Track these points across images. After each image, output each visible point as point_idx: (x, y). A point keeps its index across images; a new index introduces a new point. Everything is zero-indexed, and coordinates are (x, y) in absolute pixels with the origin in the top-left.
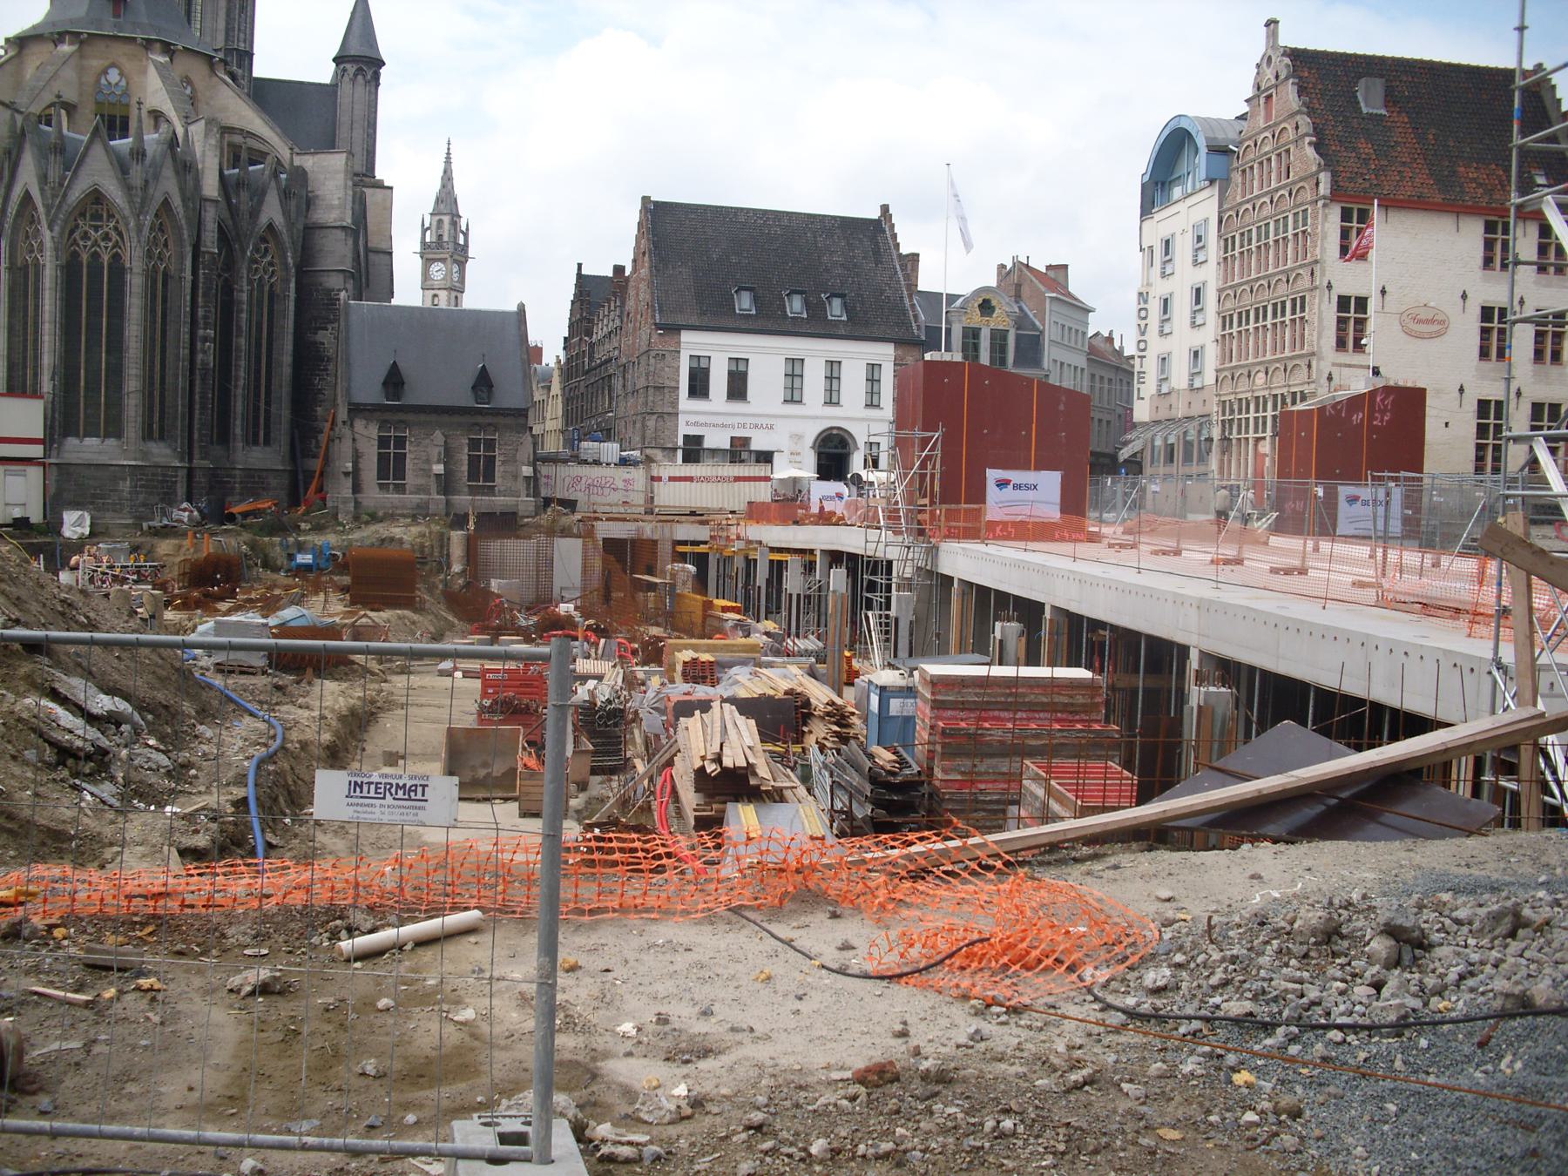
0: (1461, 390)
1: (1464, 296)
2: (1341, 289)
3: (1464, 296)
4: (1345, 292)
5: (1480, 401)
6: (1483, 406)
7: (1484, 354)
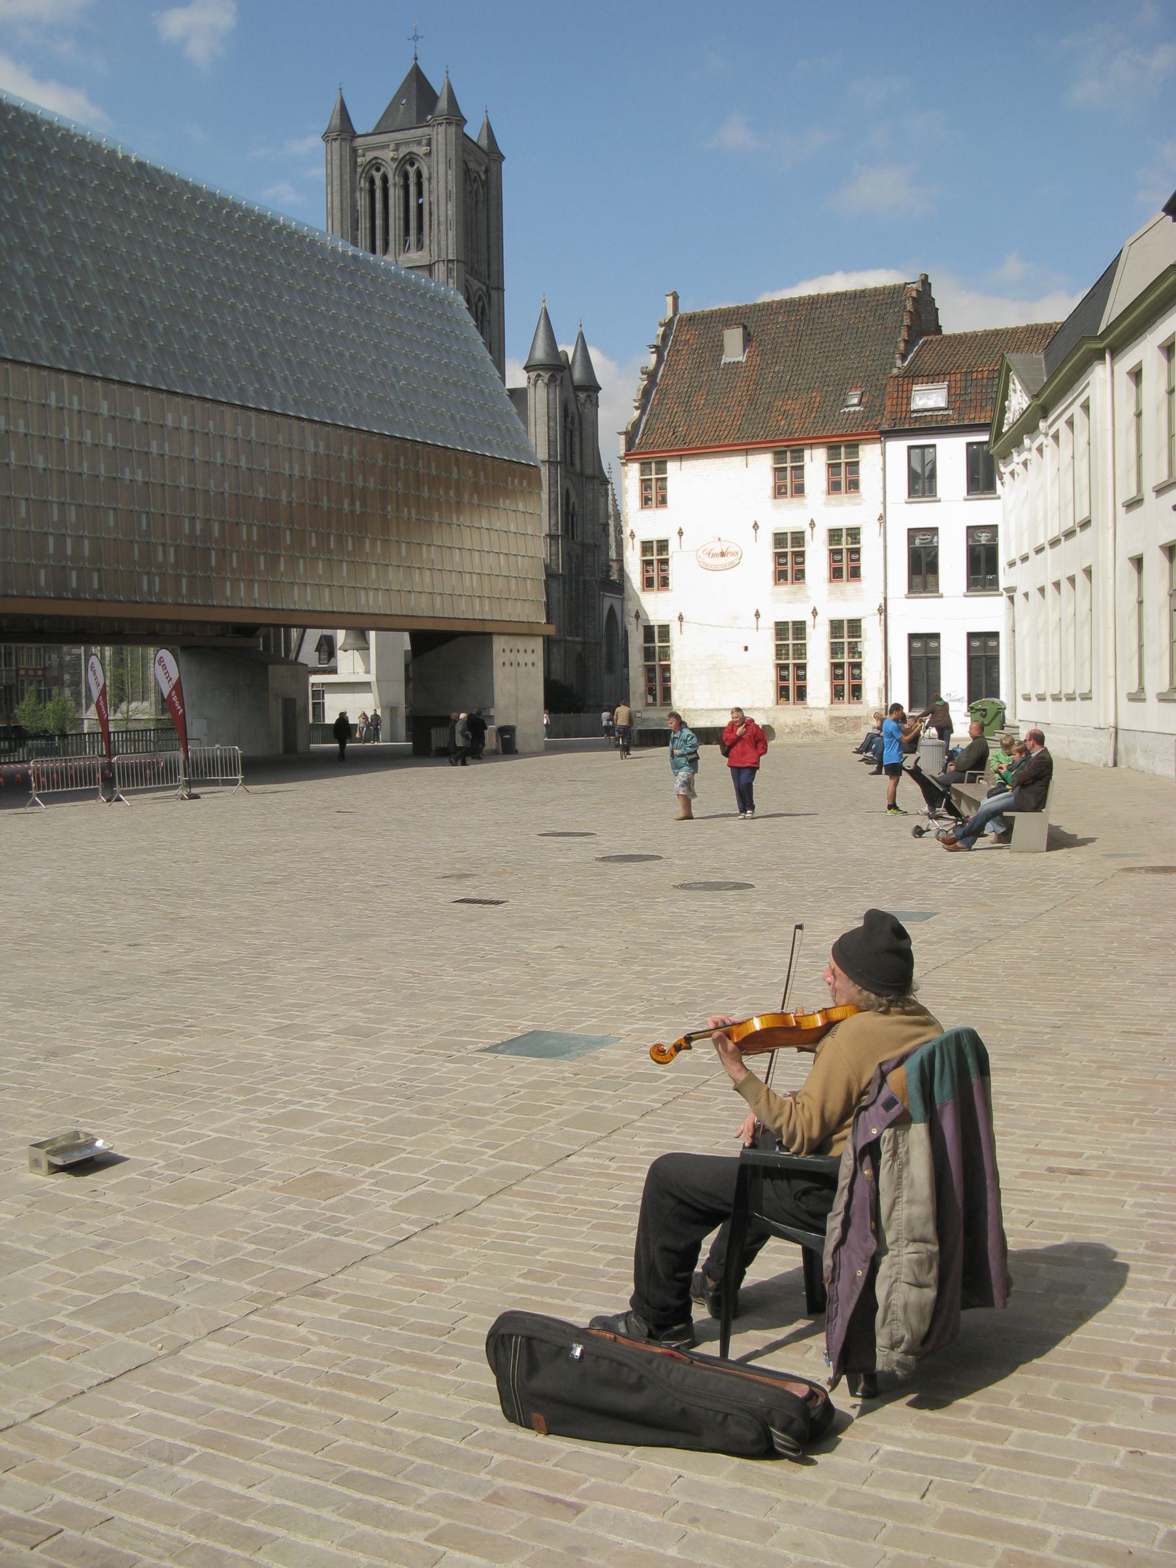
0: (757, 615)
1: (756, 526)
2: (644, 534)
3: (756, 526)
4: (647, 537)
5: (777, 624)
6: (781, 629)
7: (780, 576)
